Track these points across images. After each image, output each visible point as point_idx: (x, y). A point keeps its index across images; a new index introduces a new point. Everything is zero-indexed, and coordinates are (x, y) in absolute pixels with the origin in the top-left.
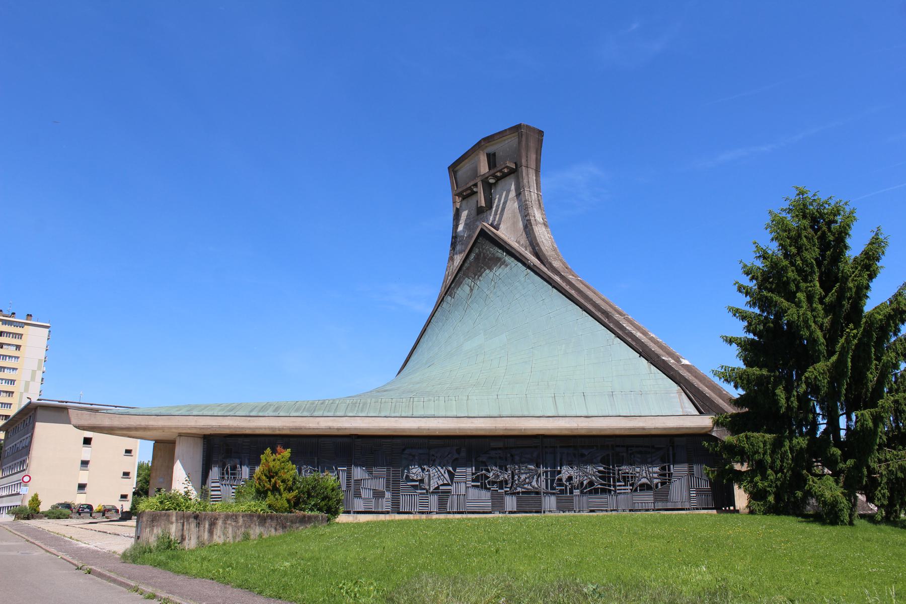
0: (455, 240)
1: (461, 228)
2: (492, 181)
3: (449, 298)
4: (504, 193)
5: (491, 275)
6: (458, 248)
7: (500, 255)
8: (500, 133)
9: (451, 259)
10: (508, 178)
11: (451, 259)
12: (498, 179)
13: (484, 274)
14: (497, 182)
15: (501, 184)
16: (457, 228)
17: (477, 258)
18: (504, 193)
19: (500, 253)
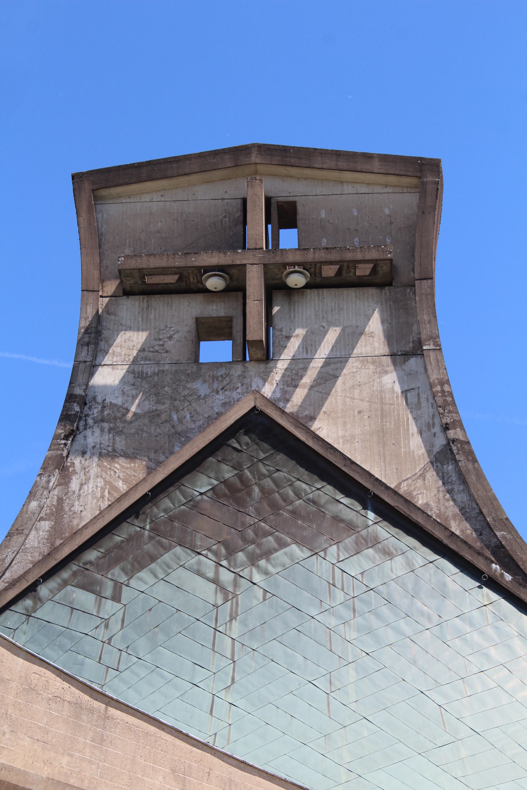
0: (77, 411)
1: (108, 377)
2: (296, 280)
3: (84, 598)
4: (332, 335)
5: (321, 566)
6: (93, 437)
7: (348, 515)
8: (338, 154)
9: (57, 465)
10: (351, 293)
11: (57, 465)
12: (317, 284)
13: (280, 555)
14: (307, 286)
15: (328, 298)
16: (92, 368)
17: (232, 494)
18: (332, 335)
19: (347, 507)
